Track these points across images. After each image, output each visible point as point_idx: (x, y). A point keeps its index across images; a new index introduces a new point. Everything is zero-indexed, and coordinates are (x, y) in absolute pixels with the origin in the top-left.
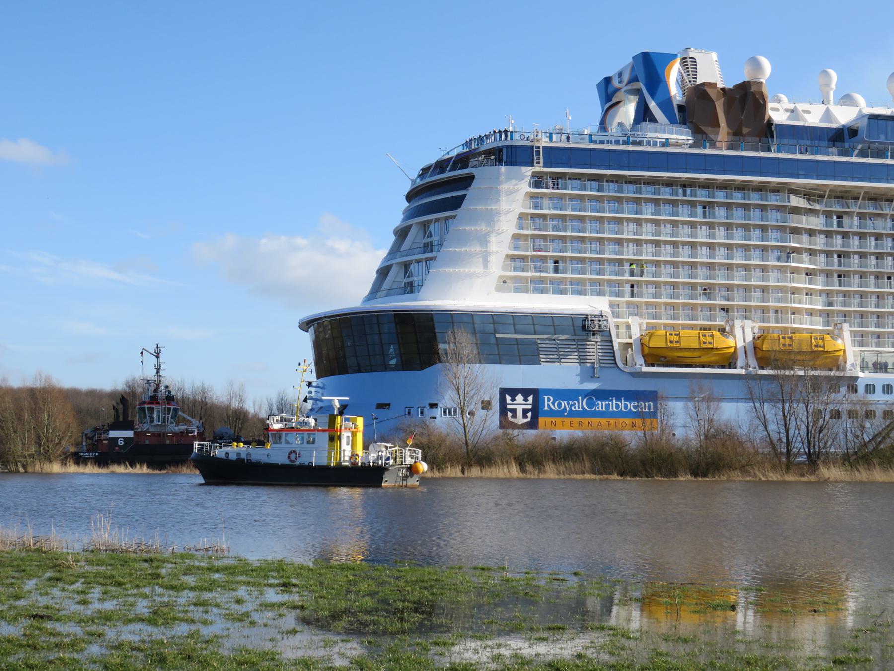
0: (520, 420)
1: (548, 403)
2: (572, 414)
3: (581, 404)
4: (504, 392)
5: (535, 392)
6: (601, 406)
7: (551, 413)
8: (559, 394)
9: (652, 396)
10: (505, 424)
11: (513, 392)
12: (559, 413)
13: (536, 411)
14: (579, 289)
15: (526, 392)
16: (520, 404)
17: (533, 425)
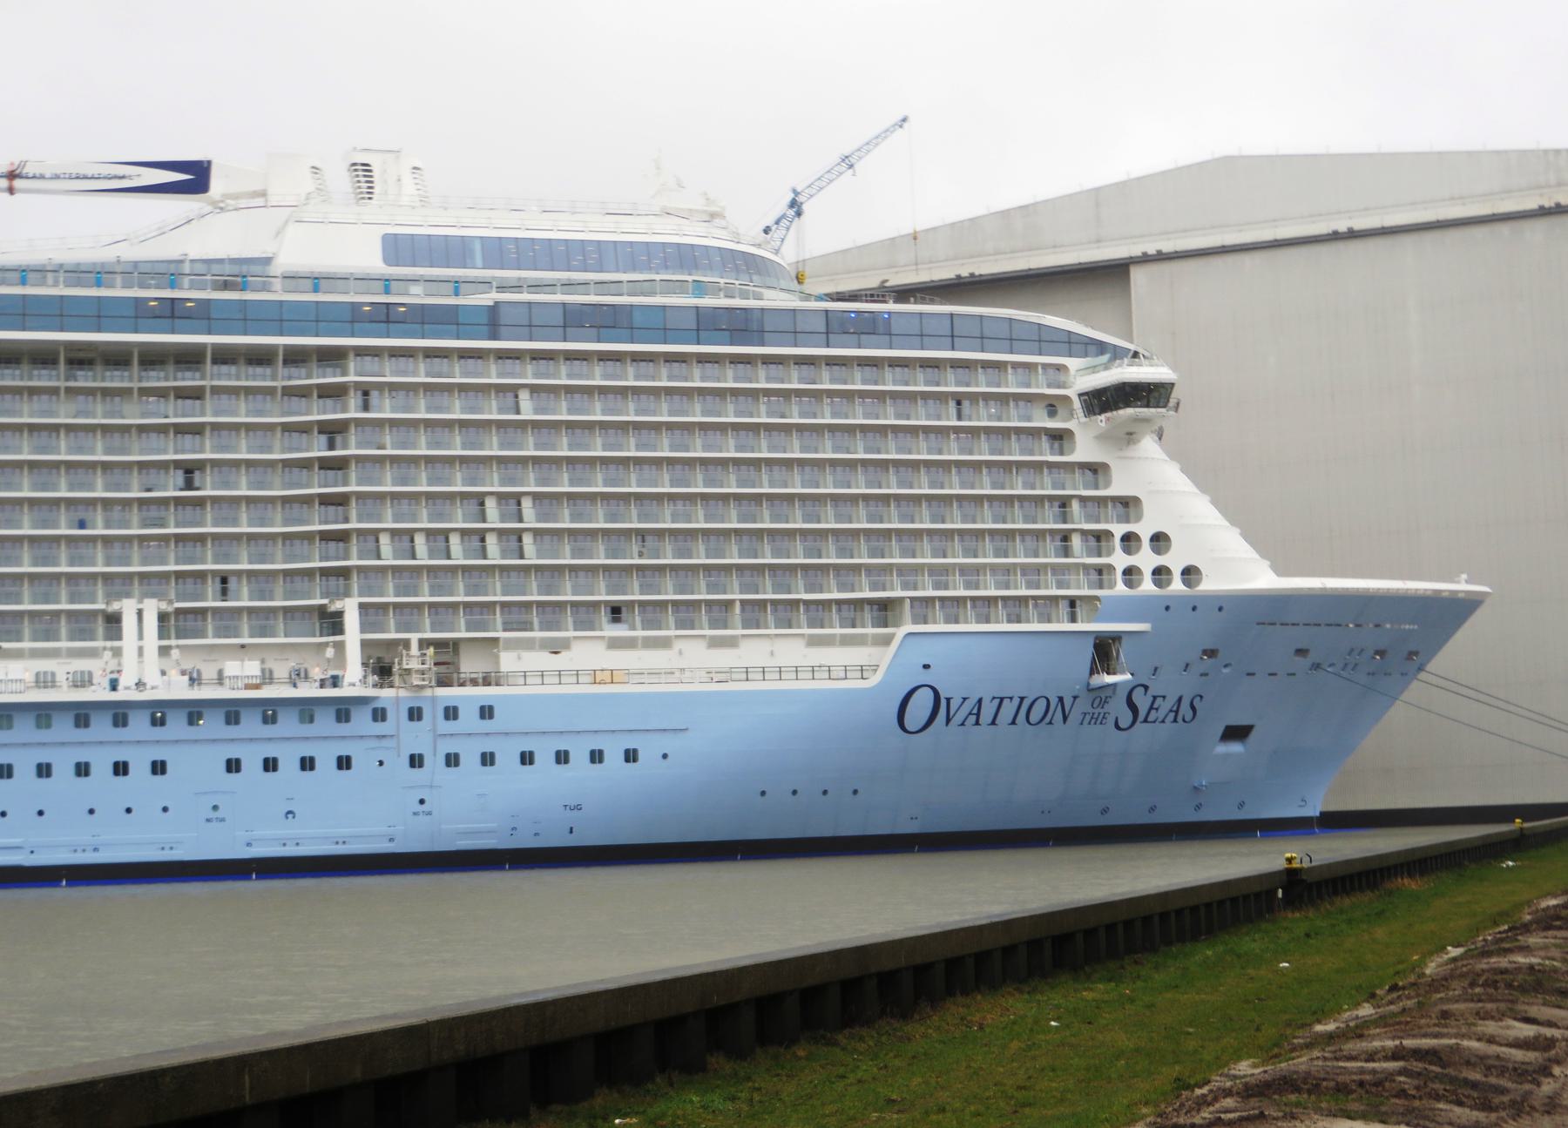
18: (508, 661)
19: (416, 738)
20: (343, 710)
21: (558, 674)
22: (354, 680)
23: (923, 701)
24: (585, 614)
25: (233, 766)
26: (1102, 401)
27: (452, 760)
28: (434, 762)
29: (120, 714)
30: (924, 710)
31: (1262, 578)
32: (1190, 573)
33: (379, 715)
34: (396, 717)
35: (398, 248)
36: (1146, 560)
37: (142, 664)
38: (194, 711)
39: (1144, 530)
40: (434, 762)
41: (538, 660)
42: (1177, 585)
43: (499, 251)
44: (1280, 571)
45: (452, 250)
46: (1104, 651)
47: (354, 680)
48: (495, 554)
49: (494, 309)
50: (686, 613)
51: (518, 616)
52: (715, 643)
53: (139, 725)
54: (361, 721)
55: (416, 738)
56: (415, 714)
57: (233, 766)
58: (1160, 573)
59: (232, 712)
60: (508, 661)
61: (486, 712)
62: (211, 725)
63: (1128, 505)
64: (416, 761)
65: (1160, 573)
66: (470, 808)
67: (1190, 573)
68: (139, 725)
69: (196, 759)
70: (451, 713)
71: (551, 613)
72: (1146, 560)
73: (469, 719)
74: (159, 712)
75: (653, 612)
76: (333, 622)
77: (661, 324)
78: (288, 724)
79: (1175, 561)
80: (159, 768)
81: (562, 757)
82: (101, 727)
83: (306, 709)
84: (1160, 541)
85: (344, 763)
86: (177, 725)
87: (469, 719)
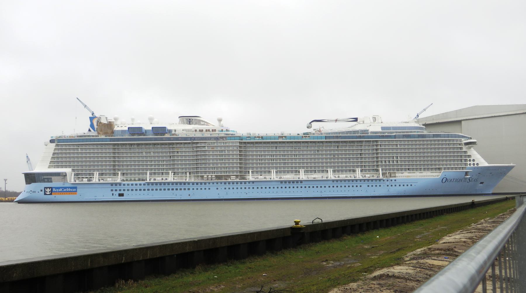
0: (48, 193)
1: (54, 190)
2: (59, 192)
3: (61, 190)
4: (45, 188)
5: (52, 188)
6: (65, 190)
7: (55, 192)
8: (56, 188)
9: (76, 188)
10: (45, 194)
11: (47, 188)
12: (56, 192)
13: (52, 191)
14: (62, 167)
15: (49, 188)
16: (48, 190)
17: (51, 194)
18: (397, 175)
19: (388, 183)
20: (380, 180)
21: (402, 176)
22: (381, 177)
23: (445, 180)
24: (405, 169)
25: (368, 186)
26: (466, 144)
27: (392, 186)
28: (390, 186)
29: (357, 180)
30: (445, 180)
31: (486, 164)
32: (477, 164)
33: (384, 181)
34: (386, 181)
35: (383, 128)
36: (472, 162)
37: (359, 175)
38: (364, 180)
39: (472, 159)
40: (390, 186)
41: (400, 175)
42: (476, 165)
43: (394, 128)
44: (489, 164)
45: (388, 128)
46: (467, 173)
47: (381, 177)
48: (395, 163)
49: (395, 135)
50: (417, 169)
51: (398, 170)
52: (420, 173)
53: (359, 182)
54: (382, 181)
55: (388, 183)
56: (388, 181)
57: (368, 186)
58: (474, 164)
59: (368, 180)
60: (397, 175)
61: (395, 180)
62: (366, 182)
63: (469, 156)
64: (388, 186)
65: (474, 164)
66: (393, 191)
67: (477, 164)
68: (359, 182)
69: (364, 186)
70: (391, 180)
71: (402, 169)
72: (472, 162)
73: (393, 181)
74: (361, 180)
75: (413, 169)
76: (377, 170)
77: (414, 136)
78: (374, 181)
79: (475, 163)
80: (361, 186)
81: (404, 185)
82: (355, 182)
83: (376, 180)
84: (474, 160)
85: (380, 186)
86: (362, 182)
87: (393, 181)
